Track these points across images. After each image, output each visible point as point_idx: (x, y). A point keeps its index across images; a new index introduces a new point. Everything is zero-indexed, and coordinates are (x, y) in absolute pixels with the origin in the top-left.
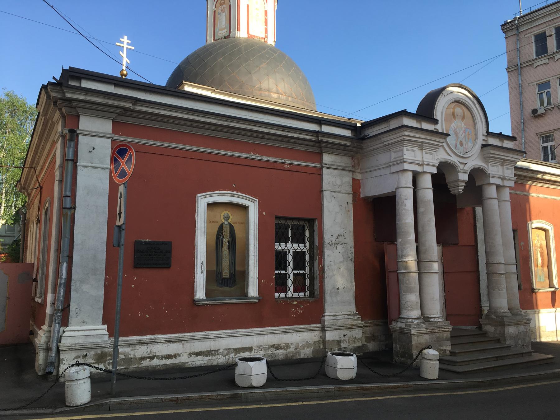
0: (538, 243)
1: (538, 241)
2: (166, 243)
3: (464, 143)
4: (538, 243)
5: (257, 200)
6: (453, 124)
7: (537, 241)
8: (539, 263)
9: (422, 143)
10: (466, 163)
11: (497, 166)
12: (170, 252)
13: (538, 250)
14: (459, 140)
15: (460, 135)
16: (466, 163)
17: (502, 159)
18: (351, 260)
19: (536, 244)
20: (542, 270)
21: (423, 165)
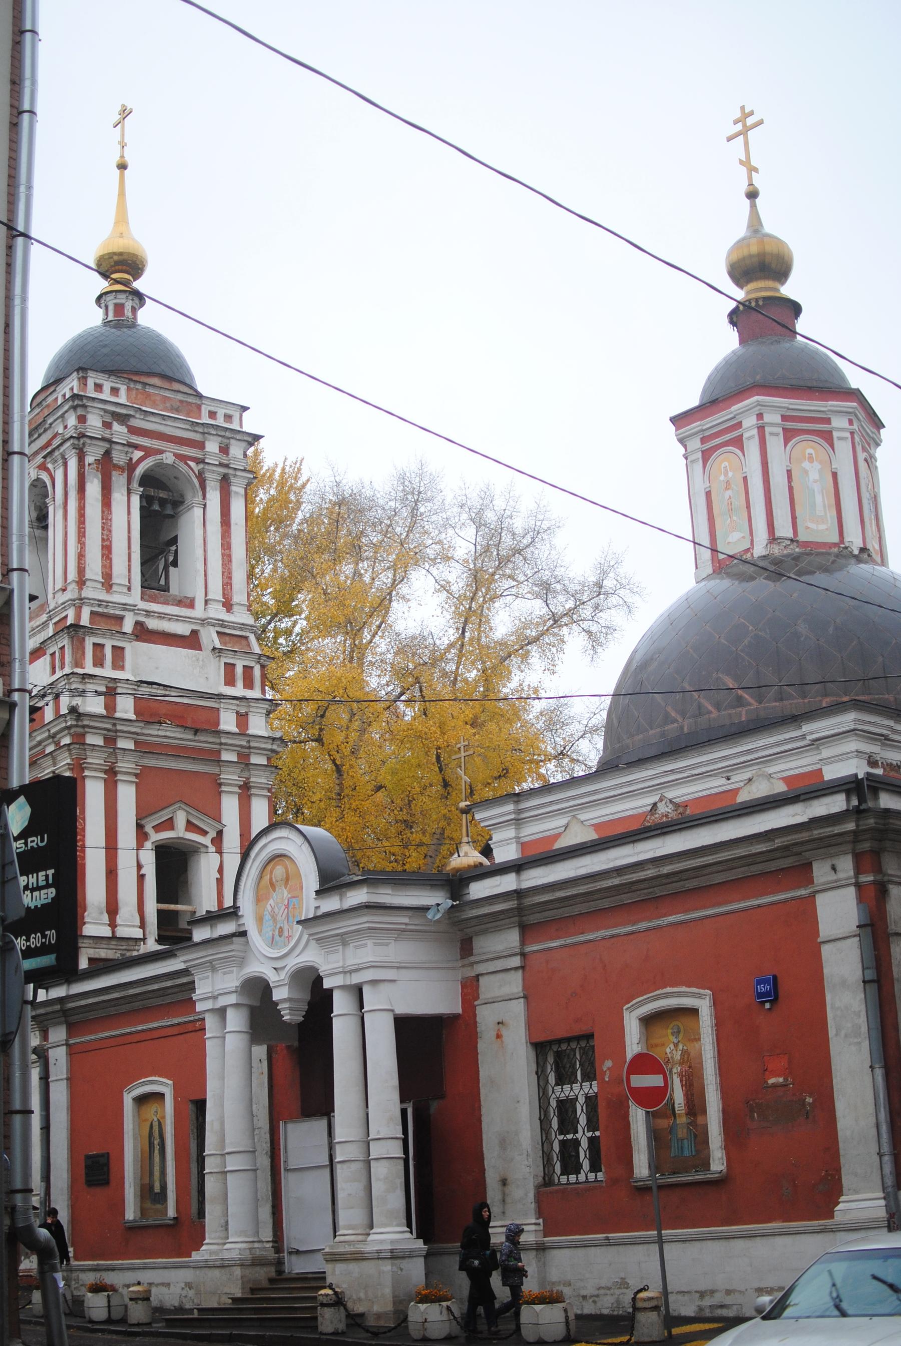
0: (674, 1052)
1: (676, 1045)
2: (102, 1156)
3: (286, 927)
4: (674, 1052)
5: (170, 1082)
6: (271, 902)
7: (672, 1046)
8: (676, 1106)
9: (210, 962)
10: (275, 968)
11: (337, 951)
12: (107, 1164)
13: (674, 1070)
14: (278, 927)
15: (279, 918)
16: (275, 968)
17: (337, 935)
18: (267, 1153)
19: (669, 1056)
20: (688, 1123)
21: (215, 998)
